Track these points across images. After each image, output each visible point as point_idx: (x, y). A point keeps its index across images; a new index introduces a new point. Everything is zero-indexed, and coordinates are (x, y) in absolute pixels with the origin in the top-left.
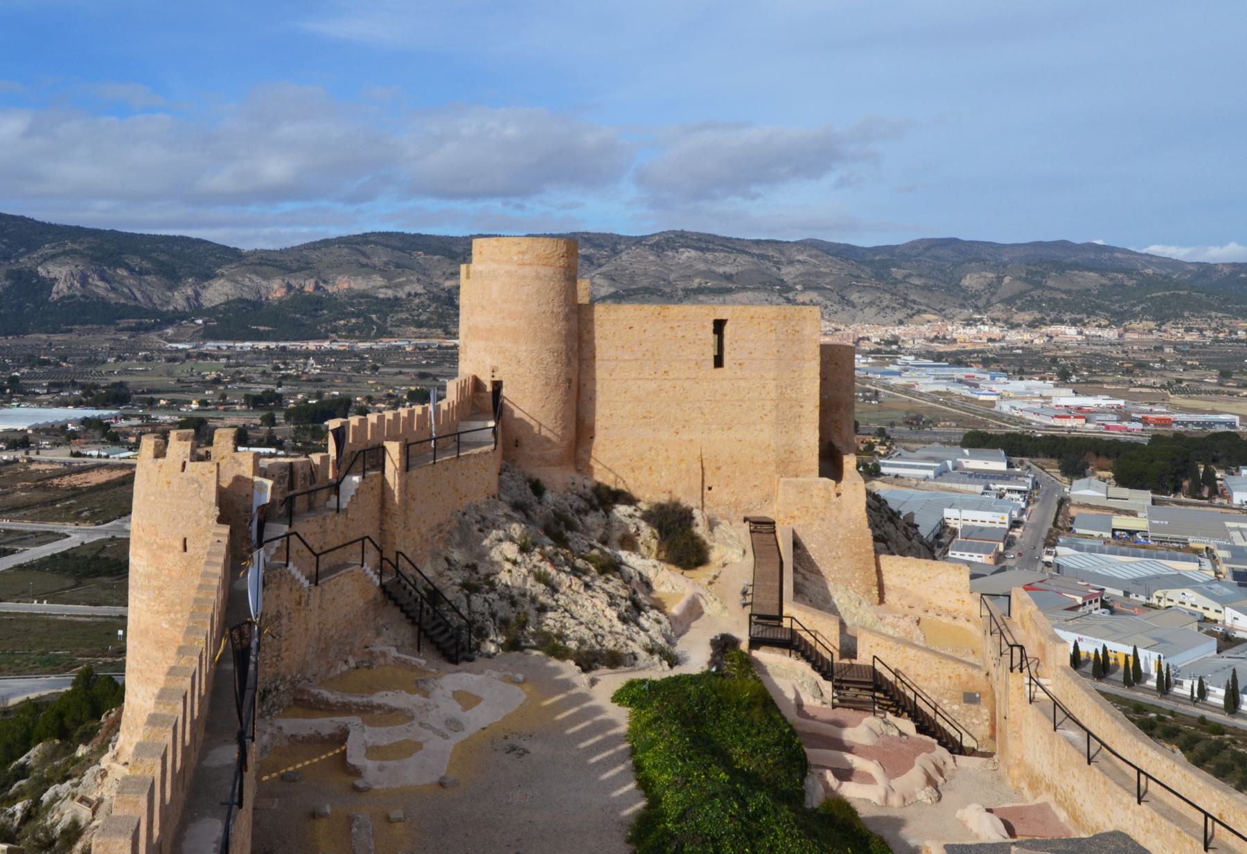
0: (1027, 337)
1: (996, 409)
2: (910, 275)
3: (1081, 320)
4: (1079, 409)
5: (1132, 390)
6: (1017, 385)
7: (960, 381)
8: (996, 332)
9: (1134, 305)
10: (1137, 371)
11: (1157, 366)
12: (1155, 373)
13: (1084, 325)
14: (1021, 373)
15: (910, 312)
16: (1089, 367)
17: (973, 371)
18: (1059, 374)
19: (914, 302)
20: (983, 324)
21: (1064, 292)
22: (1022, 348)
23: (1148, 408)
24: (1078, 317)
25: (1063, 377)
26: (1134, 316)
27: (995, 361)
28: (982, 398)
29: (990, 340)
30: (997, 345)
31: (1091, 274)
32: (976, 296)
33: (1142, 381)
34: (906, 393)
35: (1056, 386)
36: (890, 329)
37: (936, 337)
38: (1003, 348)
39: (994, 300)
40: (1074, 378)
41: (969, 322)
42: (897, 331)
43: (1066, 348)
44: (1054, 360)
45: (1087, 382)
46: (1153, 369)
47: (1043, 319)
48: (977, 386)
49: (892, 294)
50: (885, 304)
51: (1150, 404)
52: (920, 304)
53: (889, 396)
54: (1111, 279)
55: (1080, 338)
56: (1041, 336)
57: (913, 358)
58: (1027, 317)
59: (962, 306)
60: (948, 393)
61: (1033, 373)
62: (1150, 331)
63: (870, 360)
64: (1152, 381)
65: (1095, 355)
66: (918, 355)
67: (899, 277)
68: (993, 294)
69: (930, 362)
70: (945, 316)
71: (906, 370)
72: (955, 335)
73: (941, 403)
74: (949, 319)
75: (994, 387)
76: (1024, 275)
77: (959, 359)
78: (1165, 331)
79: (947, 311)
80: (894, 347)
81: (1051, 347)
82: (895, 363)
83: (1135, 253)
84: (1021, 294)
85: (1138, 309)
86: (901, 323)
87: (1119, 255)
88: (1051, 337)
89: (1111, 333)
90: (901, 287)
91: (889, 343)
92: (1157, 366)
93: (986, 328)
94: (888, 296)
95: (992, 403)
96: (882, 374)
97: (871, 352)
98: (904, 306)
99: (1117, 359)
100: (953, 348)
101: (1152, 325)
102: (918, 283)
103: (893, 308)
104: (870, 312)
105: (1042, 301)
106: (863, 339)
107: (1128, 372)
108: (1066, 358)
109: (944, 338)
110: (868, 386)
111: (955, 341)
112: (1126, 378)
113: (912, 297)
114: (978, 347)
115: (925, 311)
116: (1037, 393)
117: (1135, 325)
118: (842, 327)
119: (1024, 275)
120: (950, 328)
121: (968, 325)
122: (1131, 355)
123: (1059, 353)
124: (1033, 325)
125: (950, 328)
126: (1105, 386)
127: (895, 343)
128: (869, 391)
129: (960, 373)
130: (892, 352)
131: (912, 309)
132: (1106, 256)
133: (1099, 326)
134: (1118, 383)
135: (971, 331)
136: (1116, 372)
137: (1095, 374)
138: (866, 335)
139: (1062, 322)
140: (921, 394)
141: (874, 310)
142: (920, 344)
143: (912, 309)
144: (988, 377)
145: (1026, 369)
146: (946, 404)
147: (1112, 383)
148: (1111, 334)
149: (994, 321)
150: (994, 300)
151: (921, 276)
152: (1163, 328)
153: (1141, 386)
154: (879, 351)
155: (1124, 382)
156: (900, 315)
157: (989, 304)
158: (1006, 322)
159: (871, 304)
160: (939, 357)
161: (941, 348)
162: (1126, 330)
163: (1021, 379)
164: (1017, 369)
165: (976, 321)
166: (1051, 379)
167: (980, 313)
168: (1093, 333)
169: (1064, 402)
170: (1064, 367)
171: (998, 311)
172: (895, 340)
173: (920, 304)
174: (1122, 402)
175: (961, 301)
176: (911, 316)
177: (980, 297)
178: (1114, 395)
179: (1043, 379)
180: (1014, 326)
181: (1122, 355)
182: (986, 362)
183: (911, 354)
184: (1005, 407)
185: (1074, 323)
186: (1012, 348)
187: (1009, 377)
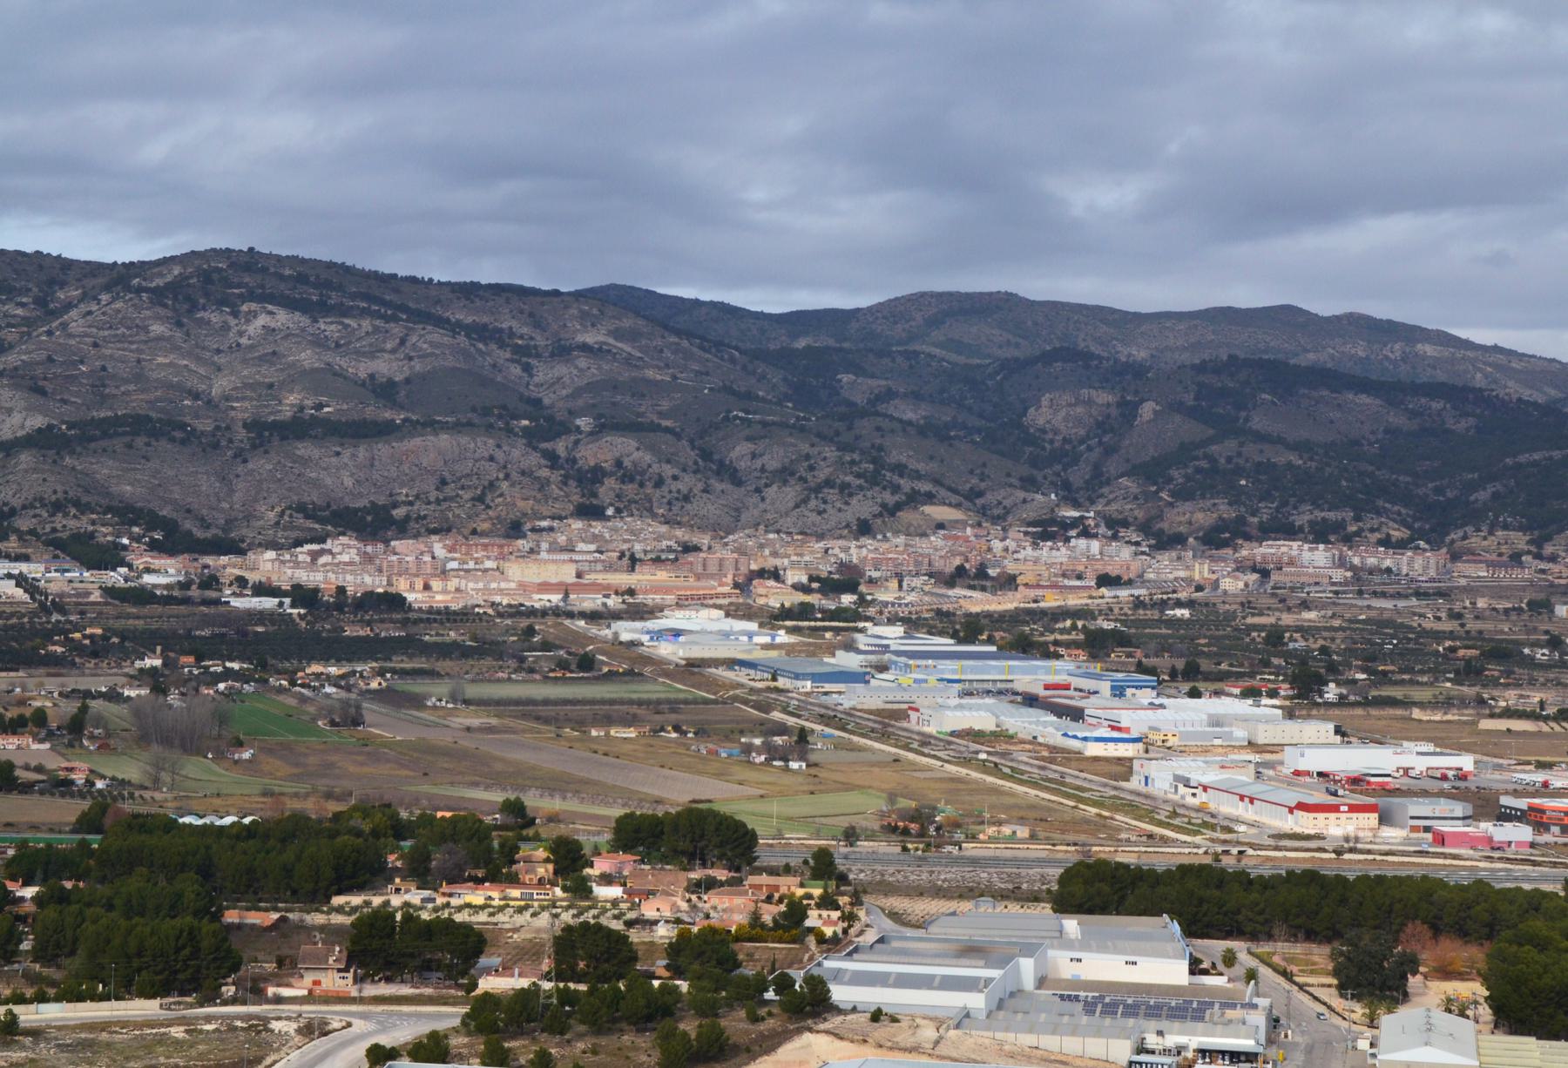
0: (1201, 570)
1: (1135, 783)
2: (889, 395)
3: (1339, 527)
4: (1356, 781)
5: (1487, 724)
6: (1185, 714)
7: (1031, 701)
8: (1121, 557)
9: (1472, 487)
10: (1493, 670)
11: (1542, 654)
12: (1540, 676)
13: (1348, 540)
14: (1192, 676)
15: (890, 498)
16: (1370, 659)
17: (1062, 670)
18: (1293, 681)
19: (900, 469)
20: (1086, 534)
21: (1296, 447)
22: (1190, 604)
23: (1539, 777)
24: (1332, 515)
25: (1305, 689)
26: (1473, 517)
27: (1119, 639)
28: (1093, 750)
29: (1105, 580)
30: (1124, 593)
31: (1364, 399)
32: (1066, 455)
33: (1509, 698)
34: (884, 736)
35: (1290, 714)
36: (836, 546)
37: (960, 571)
38: (1138, 603)
39: (1112, 467)
40: (1332, 692)
41: (1049, 530)
42: (858, 552)
43: (1305, 605)
44: (1275, 637)
45: (1367, 703)
46: (1531, 663)
47: (1241, 520)
48: (1077, 715)
49: (843, 448)
50: (822, 475)
51: (1541, 766)
52: (918, 476)
53: (839, 745)
54: (1414, 414)
55: (1339, 575)
56: (1240, 568)
57: (899, 630)
58: (1201, 515)
59: (1029, 484)
60: (1000, 736)
61: (1222, 677)
62: (1516, 558)
63: (782, 637)
64: (1536, 697)
65: (1381, 624)
66: (913, 624)
67: (859, 399)
68: (1109, 451)
69: (944, 643)
70: (983, 511)
71: (882, 668)
72: (1011, 568)
73: (983, 767)
74: (995, 520)
75: (1126, 718)
76: (1189, 399)
77: (1023, 636)
78: (1553, 559)
79: (990, 498)
80: (847, 599)
81: (1265, 601)
82: (850, 647)
83: (1467, 344)
84: (1186, 452)
85: (1482, 496)
86: (864, 529)
87: (1429, 349)
88: (1265, 574)
89: (1419, 562)
90: (864, 426)
91: (831, 587)
92: (1542, 654)
93: (1095, 546)
94: (830, 452)
95: (1123, 768)
96: (817, 678)
97: (785, 614)
98: (873, 480)
99: (1438, 636)
100: (1007, 603)
101: (1520, 540)
102: (909, 415)
103: (844, 487)
104: (782, 496)
105: (1239, 472)
106: (762, 574)
107: (1469, 672)
108: (1305, 631)
109: (981, 573)
110: (776, 715)
111: (1009, 582)
112: (1468, 691)
113: (895, 457)
114: (1074, 601)
115: (930, 498)
116: (1240, 734)
117: (1475, 541)
118: (704, 540)
119: (1189, 399)
120: (997, 545)
121: (1046, 536)
122: (1473, 626)
123: (1287, 619)
124: (1215, 539)
125: (997, 545)
126: (1417, 713)
127: (851, 587)
128: (782, 730)
129: (1031, 674)
130: (838, 614)
131: (896, 489)
132: (1396, 349)
133: (1386, 542)
134: (1447, 703)
135: (1055, 555)
136: (1437, 673)
137: (1383, 678)
138: (771, 563)
139: (1291, 532)
140: (926, 740)
141: (791, 493)
142: (916, 595)
143: (896, 489)
144: (1105, 687)
145: (1205, 665)
146: (996, 770)
147: (1433, 705)
148: (1420, 564)
149: (1115, 526)
150: (1112, 467)
151: (917, 397)
152: (1548, 549)
153: (1508, 713)
154: (804, 611)
155: (1463, 703)
156: (863, 507)
157: (1097, 482)
158: (1145, 528)
159: (784, 474)
160: (970, 629)
161: (977, 602)
162: (1455, 557)
163: (1194, 694)
164: (1180, 664)
165: (1066, 525)
166: (1273, 694)
167: (1076, 505)
168: (1372, 561)
169: (1316, 760)
170: (1303, 658)
171: (1124, 494)
172: (847, 579)
173: (918, 476)
174: (1466, 762)
175: (1025, 470)
176: (891, 511)
177: (1075, 461)
178: (1445, 741)
179: (1251, 693)
180: (1166, 541)
181: (1447, 626)
182: (1097, 645)
183: (891, 621)
184: (1159, 778)
185: (1320, 534)
186: (1163, 605)
187: (1159, 687)
